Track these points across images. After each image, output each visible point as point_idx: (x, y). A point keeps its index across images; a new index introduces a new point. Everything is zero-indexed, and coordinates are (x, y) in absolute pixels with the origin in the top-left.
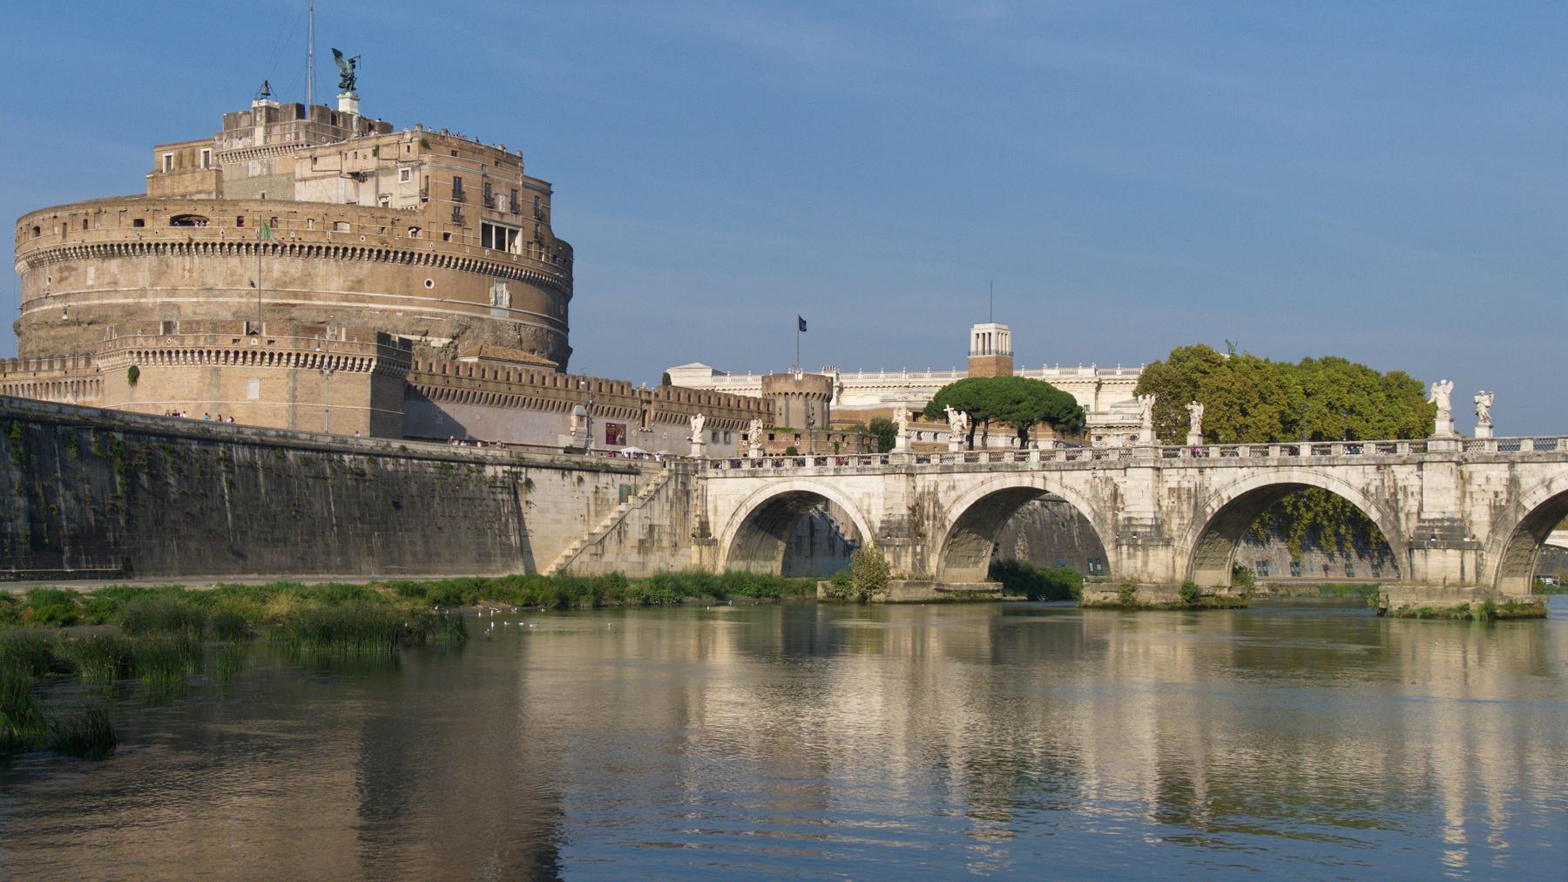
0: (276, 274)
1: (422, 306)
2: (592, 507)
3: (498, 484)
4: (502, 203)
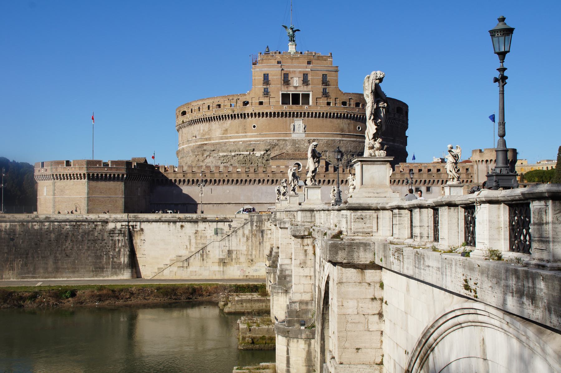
0: (201, 131)
1: (252, 137)
2: (193, 241)
3: (117, 232)
4: (296, 81)
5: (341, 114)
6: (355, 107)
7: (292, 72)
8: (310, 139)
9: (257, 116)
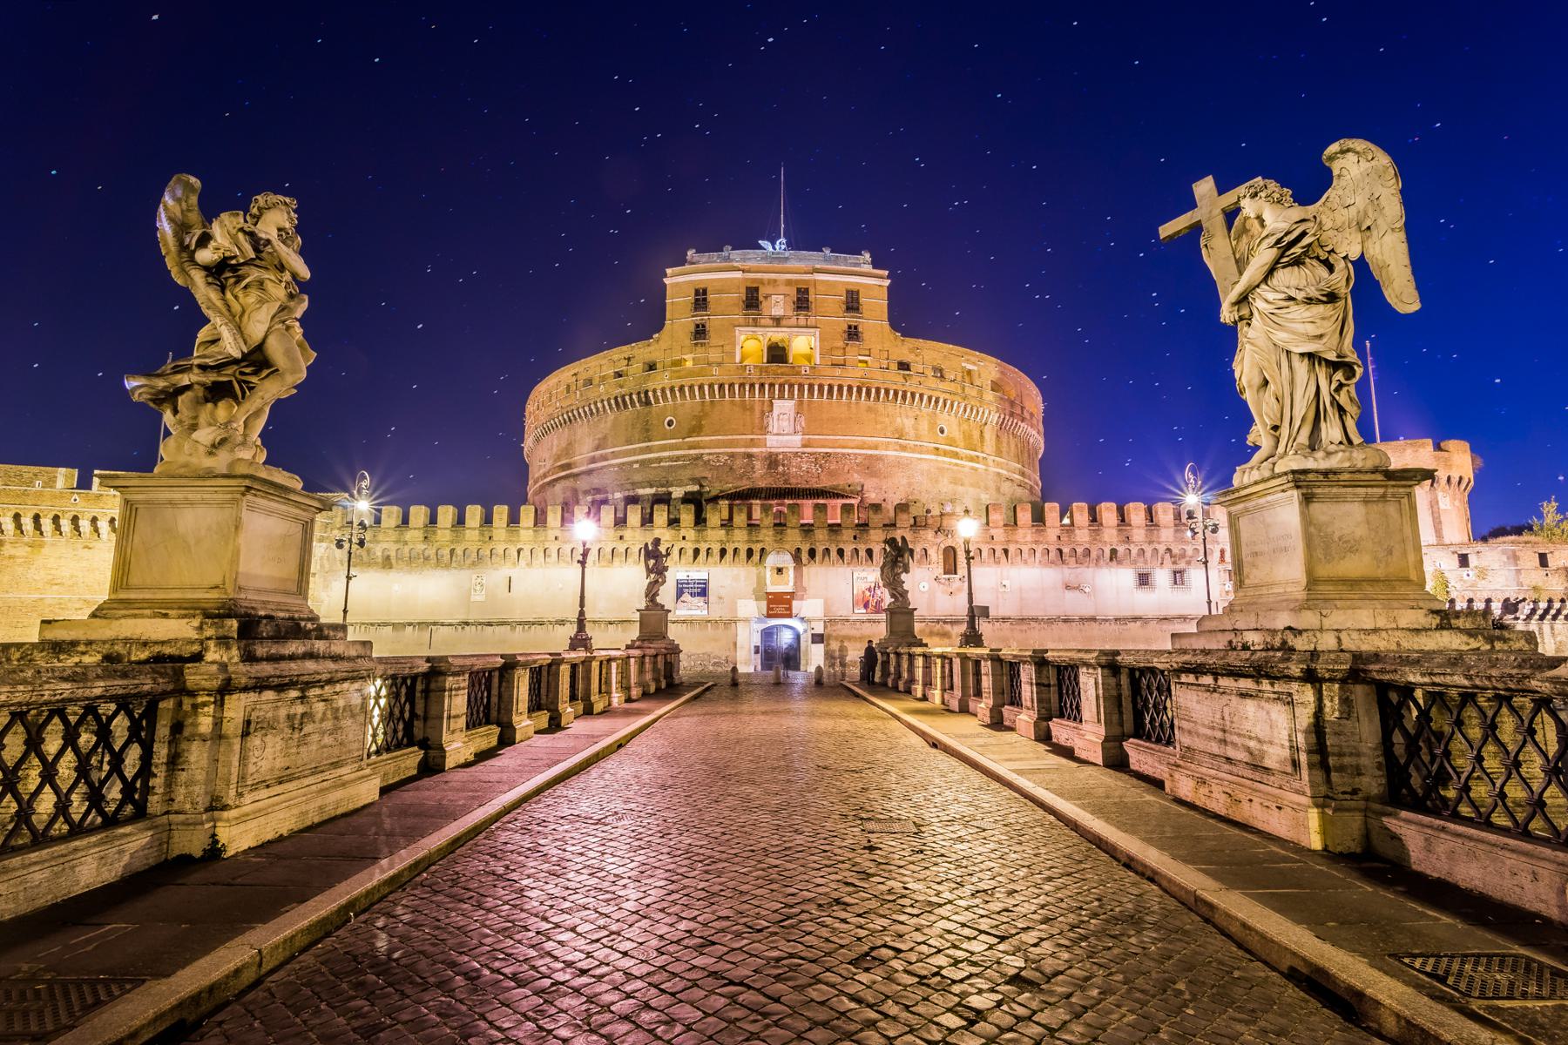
0: (555, 449)
4: (778, 305)
5: (896, 393)
6: (930, 373)
7: (769, 283)
8: (815, 453)
9: (678, 394)
